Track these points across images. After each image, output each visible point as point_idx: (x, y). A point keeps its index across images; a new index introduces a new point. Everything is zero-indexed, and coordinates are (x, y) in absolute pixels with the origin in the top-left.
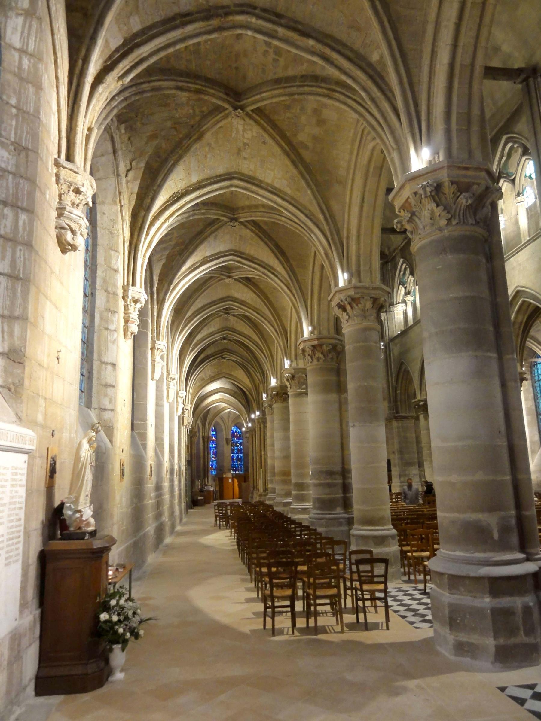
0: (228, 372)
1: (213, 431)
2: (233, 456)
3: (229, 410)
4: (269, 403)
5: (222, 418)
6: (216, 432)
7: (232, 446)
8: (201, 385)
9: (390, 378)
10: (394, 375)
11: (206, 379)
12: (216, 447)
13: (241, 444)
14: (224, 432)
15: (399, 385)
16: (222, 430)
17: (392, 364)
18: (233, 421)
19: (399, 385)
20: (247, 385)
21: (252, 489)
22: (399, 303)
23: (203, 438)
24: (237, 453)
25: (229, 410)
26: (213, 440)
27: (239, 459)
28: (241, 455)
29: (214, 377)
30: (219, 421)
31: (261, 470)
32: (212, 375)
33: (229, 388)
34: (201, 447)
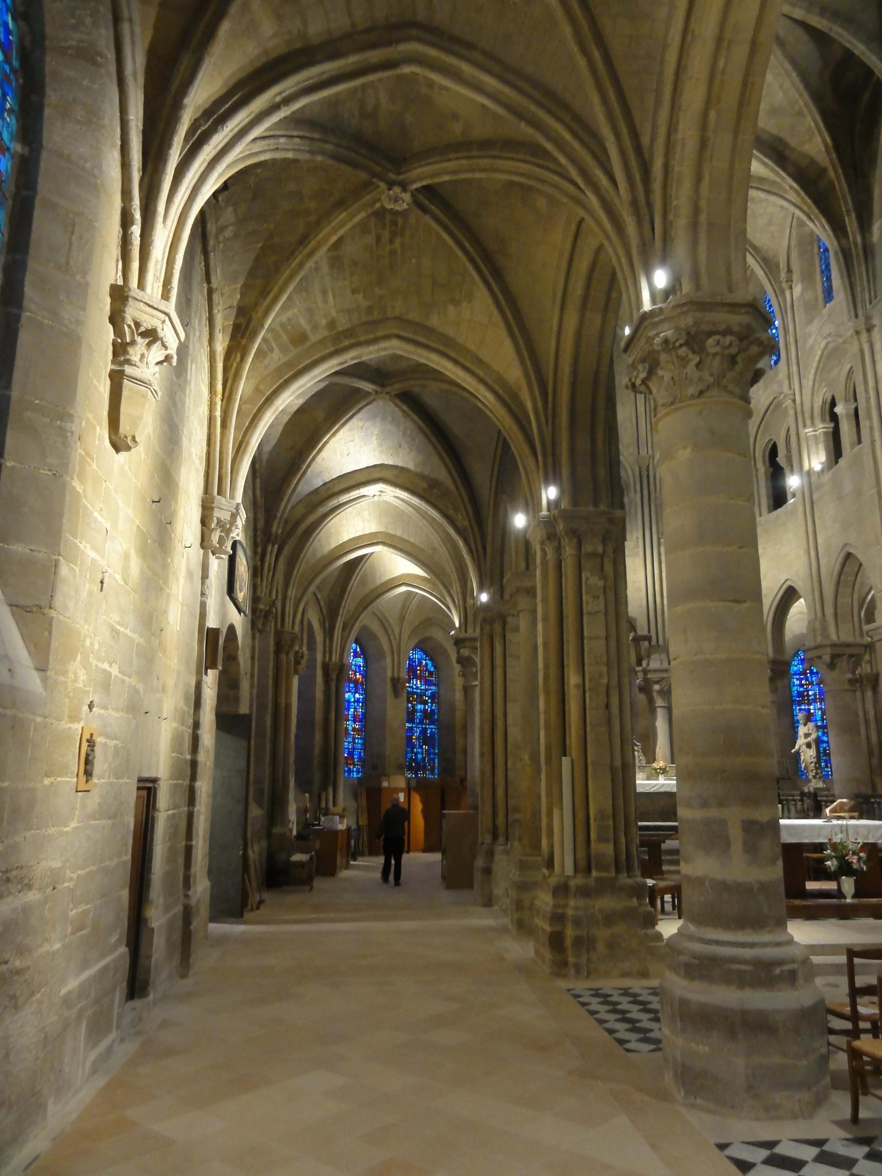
0: (414, 316)
1: (356, 655)
2: (411, 729)
3: (403, 589)
4: (688, 321)
5: (383, 622)
6: (366, 660)
7: (409, 701)
8: (289, 365)
11: (314, 338)
12: (365, 702)
13: (432, 697)
14: (389, 660)
16: (382, 656)
18: (414, 632)
20: (501, 380)
21: (488, 839)
23: (326, 667)
24: (421, 722)
25: (403, 589)
26: (356, 682)
27: (426, 739)
28: (431, 729)
29: (348, 333)
30: (375, 627)
31: (566, 761)
32: (343, 324)
33: (411, 466)
34: (319, 694)
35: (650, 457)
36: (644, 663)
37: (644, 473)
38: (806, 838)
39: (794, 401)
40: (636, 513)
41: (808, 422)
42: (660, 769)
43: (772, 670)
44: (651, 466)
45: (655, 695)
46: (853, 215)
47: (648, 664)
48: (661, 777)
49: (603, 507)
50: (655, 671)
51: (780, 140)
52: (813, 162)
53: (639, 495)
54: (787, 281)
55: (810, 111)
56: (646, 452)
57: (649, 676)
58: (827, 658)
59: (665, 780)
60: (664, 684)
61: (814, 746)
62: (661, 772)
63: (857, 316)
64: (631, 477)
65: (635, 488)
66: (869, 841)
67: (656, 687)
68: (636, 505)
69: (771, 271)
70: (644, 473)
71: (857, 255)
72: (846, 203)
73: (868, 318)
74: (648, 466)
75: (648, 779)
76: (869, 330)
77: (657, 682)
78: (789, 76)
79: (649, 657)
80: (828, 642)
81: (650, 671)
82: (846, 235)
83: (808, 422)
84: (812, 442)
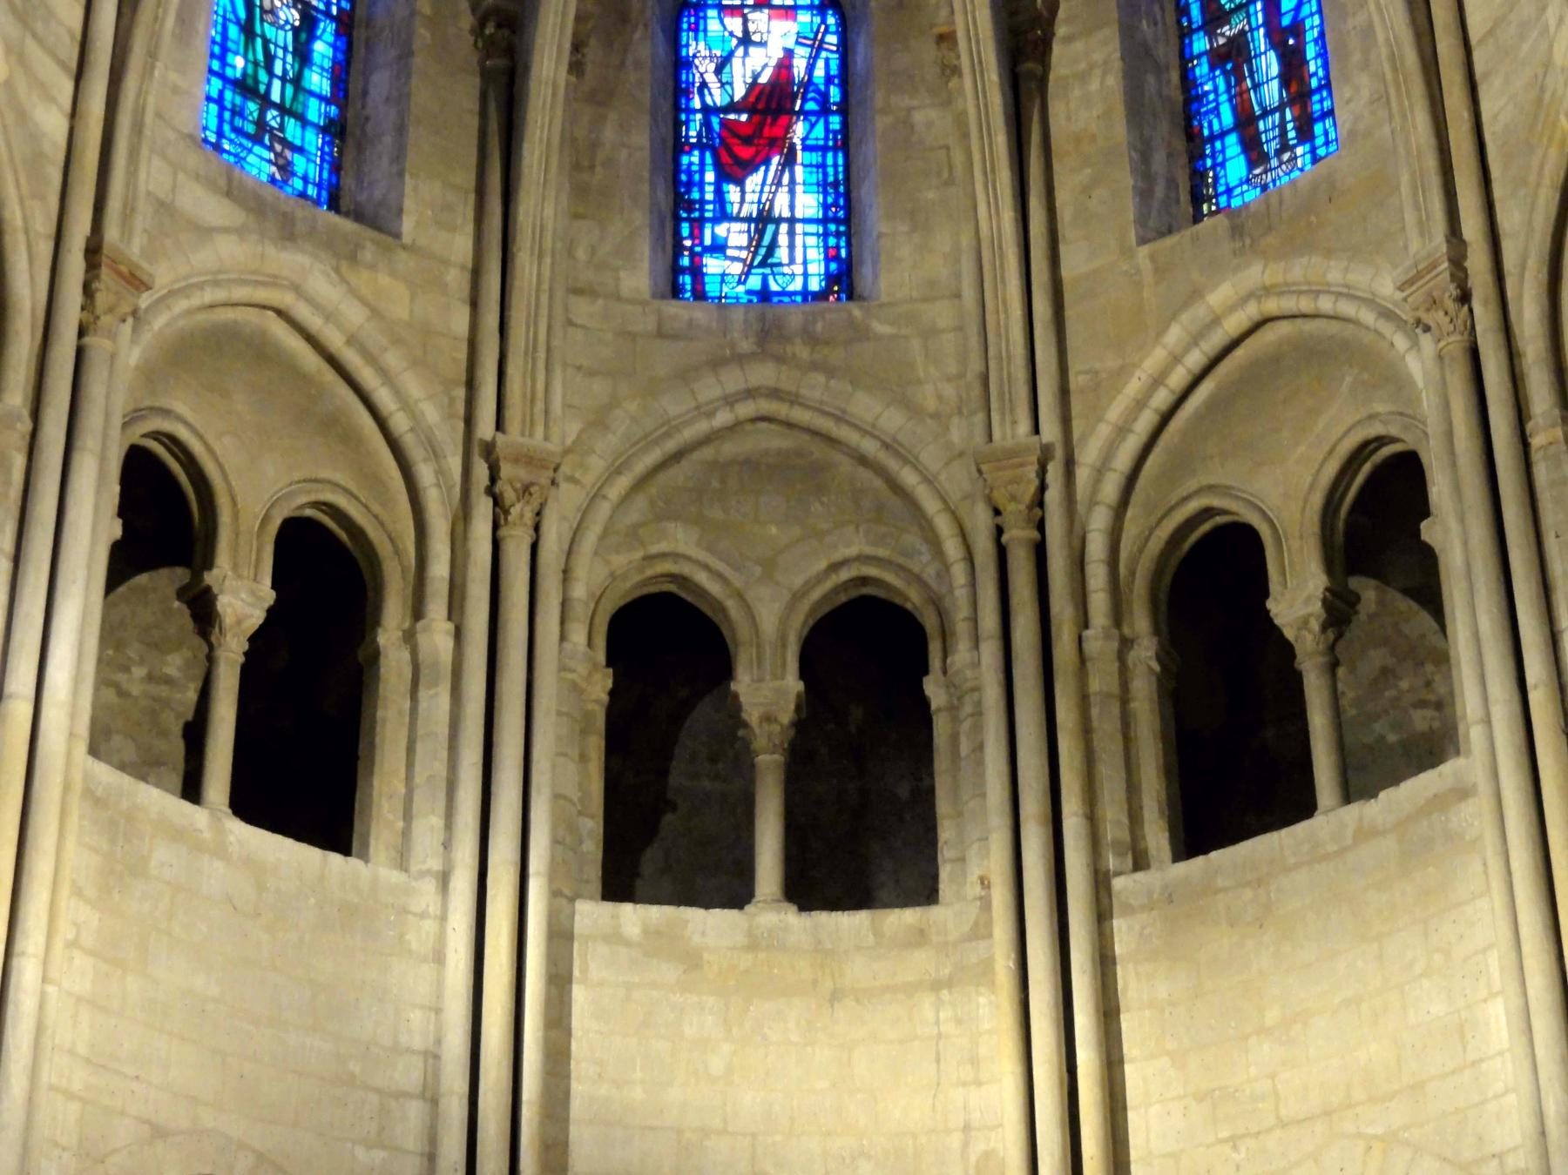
40: (980, 748)
44: (1053, 496)
53: (990, 652)
56: (1024, 426)
64: (959, 574)
65: (974, 620)
68: (978, 713)
70: (1018, 535)
74: (1039, 502)
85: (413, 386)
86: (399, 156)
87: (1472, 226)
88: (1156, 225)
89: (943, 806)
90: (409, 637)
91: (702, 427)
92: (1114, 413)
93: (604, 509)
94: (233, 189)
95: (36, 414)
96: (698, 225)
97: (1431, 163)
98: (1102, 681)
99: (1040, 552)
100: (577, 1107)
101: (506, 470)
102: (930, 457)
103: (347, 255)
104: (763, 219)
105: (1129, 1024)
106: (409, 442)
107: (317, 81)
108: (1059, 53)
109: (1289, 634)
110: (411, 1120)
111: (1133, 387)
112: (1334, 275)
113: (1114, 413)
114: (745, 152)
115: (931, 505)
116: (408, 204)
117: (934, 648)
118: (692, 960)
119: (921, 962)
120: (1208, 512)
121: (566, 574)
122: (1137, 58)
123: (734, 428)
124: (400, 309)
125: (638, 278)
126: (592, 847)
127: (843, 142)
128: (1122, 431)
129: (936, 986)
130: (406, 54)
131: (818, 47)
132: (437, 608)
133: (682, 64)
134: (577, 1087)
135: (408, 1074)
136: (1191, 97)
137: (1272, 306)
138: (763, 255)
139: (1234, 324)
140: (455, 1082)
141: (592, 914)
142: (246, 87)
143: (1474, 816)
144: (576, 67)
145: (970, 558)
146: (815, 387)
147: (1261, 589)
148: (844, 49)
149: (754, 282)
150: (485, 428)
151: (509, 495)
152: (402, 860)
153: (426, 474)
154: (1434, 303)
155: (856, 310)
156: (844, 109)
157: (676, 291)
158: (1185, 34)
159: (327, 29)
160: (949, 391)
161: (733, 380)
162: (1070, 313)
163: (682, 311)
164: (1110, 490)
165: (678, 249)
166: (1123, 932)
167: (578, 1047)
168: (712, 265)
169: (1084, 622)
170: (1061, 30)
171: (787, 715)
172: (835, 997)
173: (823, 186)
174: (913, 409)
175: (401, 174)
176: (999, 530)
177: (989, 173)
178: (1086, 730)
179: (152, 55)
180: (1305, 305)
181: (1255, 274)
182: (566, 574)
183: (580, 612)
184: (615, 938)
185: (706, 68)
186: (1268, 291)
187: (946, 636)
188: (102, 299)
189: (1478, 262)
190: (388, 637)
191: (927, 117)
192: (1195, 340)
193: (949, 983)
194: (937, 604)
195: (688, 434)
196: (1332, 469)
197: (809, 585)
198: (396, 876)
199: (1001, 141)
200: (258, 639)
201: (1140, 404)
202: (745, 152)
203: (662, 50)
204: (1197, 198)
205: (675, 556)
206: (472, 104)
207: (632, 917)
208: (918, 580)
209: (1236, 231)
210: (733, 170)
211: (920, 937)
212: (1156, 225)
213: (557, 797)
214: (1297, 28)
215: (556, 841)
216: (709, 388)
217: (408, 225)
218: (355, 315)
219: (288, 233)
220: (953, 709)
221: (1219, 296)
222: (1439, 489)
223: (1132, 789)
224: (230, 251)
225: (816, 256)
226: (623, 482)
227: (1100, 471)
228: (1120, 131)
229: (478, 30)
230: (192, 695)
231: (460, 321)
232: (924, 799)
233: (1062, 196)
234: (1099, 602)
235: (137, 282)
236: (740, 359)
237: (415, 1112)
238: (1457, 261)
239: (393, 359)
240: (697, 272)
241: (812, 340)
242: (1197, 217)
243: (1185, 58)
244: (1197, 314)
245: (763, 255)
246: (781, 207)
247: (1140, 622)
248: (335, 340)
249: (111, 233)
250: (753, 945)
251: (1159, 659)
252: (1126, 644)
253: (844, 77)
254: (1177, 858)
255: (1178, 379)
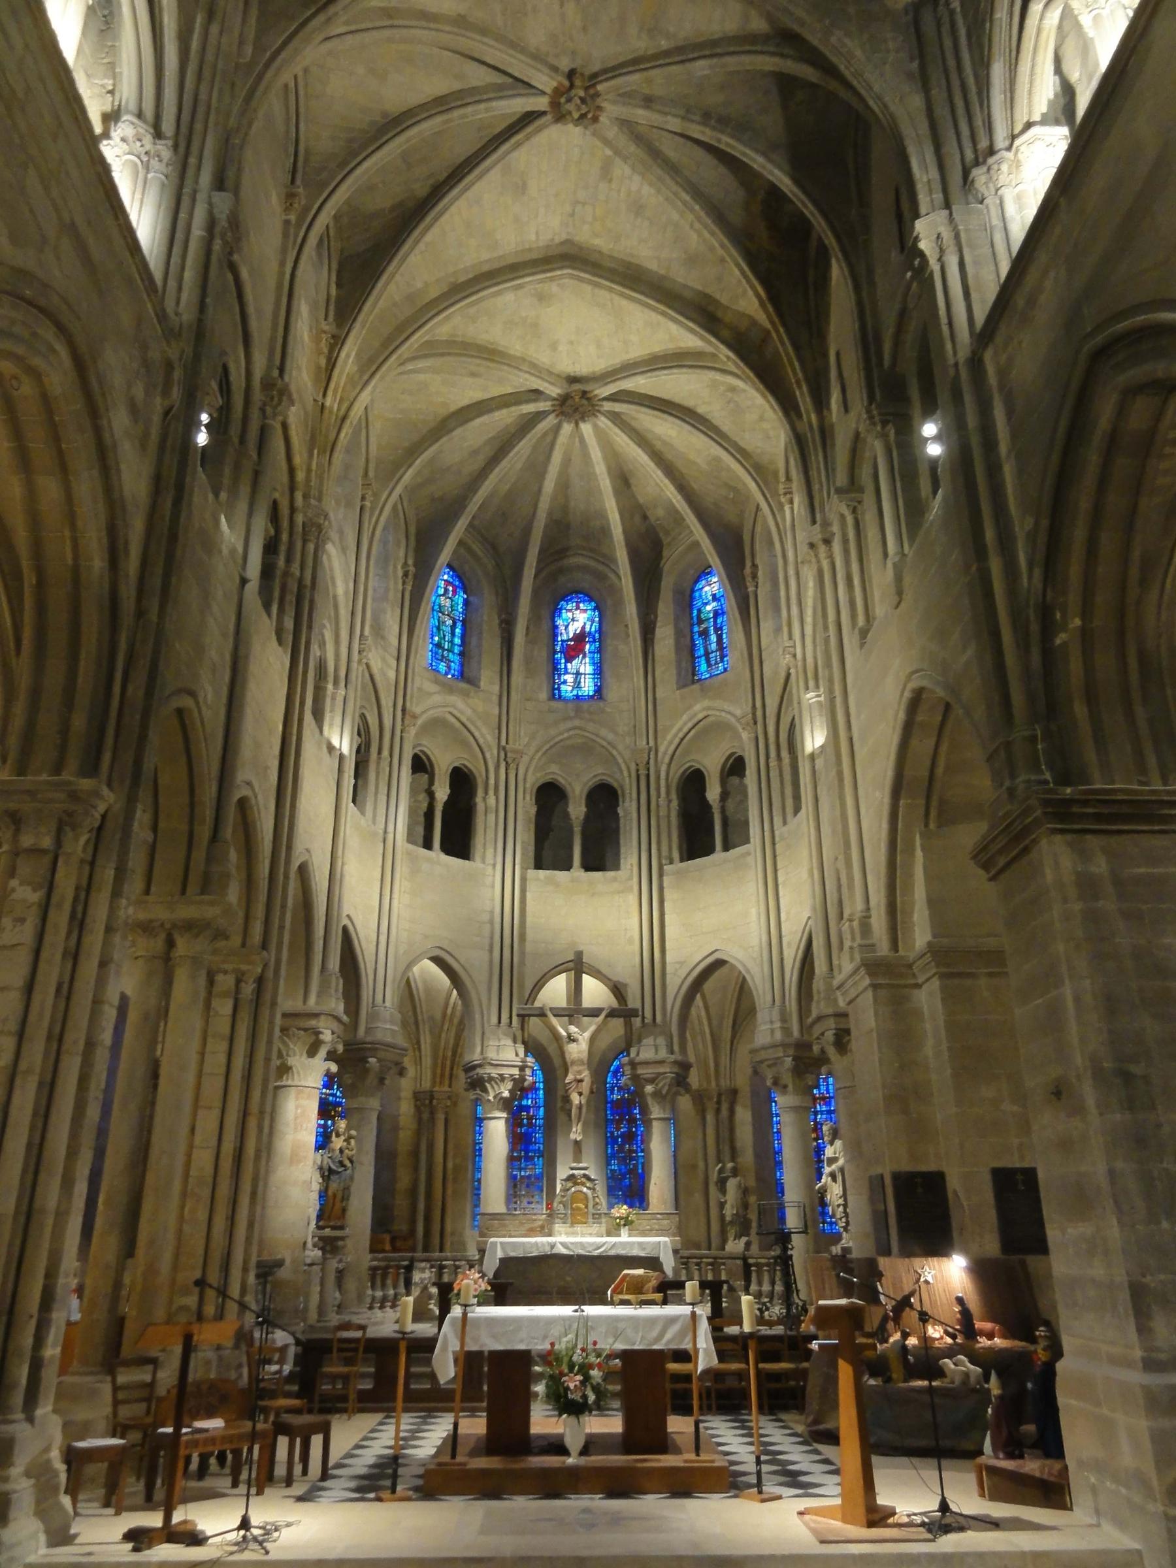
9: (995, 566)
10: (1022, 525)
15: (1075, 572)
17: (1008, 472)
19: (1075, 572)
22: (1029, 125)
35: (650, 750)
36: (633, 1052)
37: (643, 772)
38: (522, 1341)
39: (794, 656)
40: (631, 829)
41: (811, 683)
42: (621, 1218)
43: (795, 1059)
44: (652, 762)
45: (650, 1100)
46: (805, 388)
47: (638, 1054)
48: (624, 1232)
49: (65, 776)
50: (647, 1063)
51: (706, 296)
52: (754, 323)
53: (634, 805)
54: (785, 494)
55: (731, 256)
56: (644, 742)
57: (640, 1071)
58: (830, 1036)
59: (630, 1236)
60: (660, 1085)
61: (839, 1179)
62: (622, 1222)
63: (814, 522)
66: (636, 1347)
67: (649, 1089)
69: (766, 482)
70: (643, 772)
71: (814, 441)
72: (794, 370)
73: (826, 524)
74: (648, 763)
75: (609, 1234)
76: (827, 542)
77: (651, 1081)
78: (692, 210)
79: (639, 1041)
80: (830, 1011)
81: (641, 1063)
82: (800, 416)
83: (811, 683)
84: (816, 713)
85: (484, 730)
86: (479, 663)
87: (758, 704)
88: (682, 685)
89: (622, 842)
90: (484, 799)
91: (561, 737)
92: (669, 737)
93: (535, 762)
94: (436, 682)
95: (391, 756)
96: (560, 675)
97: (749, 685)
98: (663, 812)
99: (648, 776)
100: (528, 924)
101: (509, 755)
102: (620, 747)
103: (466, 695)
104: (578, 674)
105: (667, 905)
106: (483, 746)
107: (457, 641)
108: (658, 631)
109: (711, 802)
110: (486, 929)
111: (674, 731)
112: (726, 707)
113: (669, 737)
114: (572, 653)
115: (620, 761)
116: (483, 678)
117: (621, 800)
118: (557, 885)
119: (615, 885)
120: (691, 767)
121: (525, 779)
122: (679, 634)
123: (569, 738)
124: (480, 709)
125: (544, 695)
126: (531, 854)
127: (600, 651)
128: (671, 743)
129: (619, 892)
130: (481, 633)
131: (593, 622)
132: (491, 792)
133: (556, 627)
134: (529, 919)
135: (485, 917)
136: (693, 645)
137: (710, 713)
138: (577, 685)
139: (700, 716)
140: (498, 919)
141: (532, 873)
142: (439, 645)
143: (750, 860)
144: (527, 634)
145: (630, 776)
146: (591, 727)
147: (705, 791)
148: (600, 622)
149: (575, 692)
150: (503, 742)
151: (509, 760)
152: (483, 861)
153: (488, 755)
154: (748, 724)
155: (601, 704)
156: (600, 640)
157: (554, 695)
158: (692, 625)
159: (459, 625)
160: (626, 728)
161: (569, 724)
162: (658, 708)
163: (554, 704)
164: (667, 760)
165: (554, 683)
166: (666, 881)
167: (528, 908)
168: (563, 687)
169: (659, 796)
170: (658, 624)
171: (582, 818)
172: (593, 895)
173: (594, 664)
174: (616, 733)
175: (480, 669)
176: (638, 770)
177: (637, 670)
178: (658, 826)
179: (416, 653)
180: (718, 713)
181: (706, 703)
182: (525, 779)
183: (528, 791)
184: (538, 879)
185: (562, 628)
186: (709, 708)
187: (623, 796)
188: (406, 722)
189: (759, 713)
190: (479, 799)
191: (622, 647)
192: (690, 720)
193: (622, 892)
194: (622, 787)
195: (557, 740)
196: (722, 761)
197: (589, 781)
198: (482, 866)
199: (641, 661)
200: (446, 803)
201: (676, 735)
202: (572, 653)
203: (550, 624)
204: (694, 674)
205: (554, 773)
206: (499, 646)
207: (542, 873)
208: (617, 780)
209: (702, 690)
210: (569, 660)
211: (615, 879)
212: (682, 685)
213: (523, 842)
214: (721, 629)
215: (523, 854)
216: (562, 727)
217: (482, 684)
218: (469, 712)
219: (451, 690)
220: (625, 816)
221: (698, 707)
222: (747, 772)
223: (670, 841)
224: (437, 699)
225: (592, 684)
226: (540, 754)
227: (665, 753)
228: (673, 655)
229: (500, 624)
230: (425, 805)
231: (496, 711)
232: (617, 831)
233: (657, 673)
234: (663, 790)
235: (415, 717)
236: (570, 718)
237: (488, 927)
238: (754, 714)
239: (479, 724)
240: (559, 689)
241: (591, 713)
242: (693, 682)
243: (692, 632)
244: (691, 712)
245: (577, 685)
246: (582, 671)
247: (674, 796)
248: (464, 719)
249: (408, 704)
250: (573, 880)
251: (679, 805)
252: (670, 801)
253: (600, 630)
254: (682, 860)
255: (685, 730)
